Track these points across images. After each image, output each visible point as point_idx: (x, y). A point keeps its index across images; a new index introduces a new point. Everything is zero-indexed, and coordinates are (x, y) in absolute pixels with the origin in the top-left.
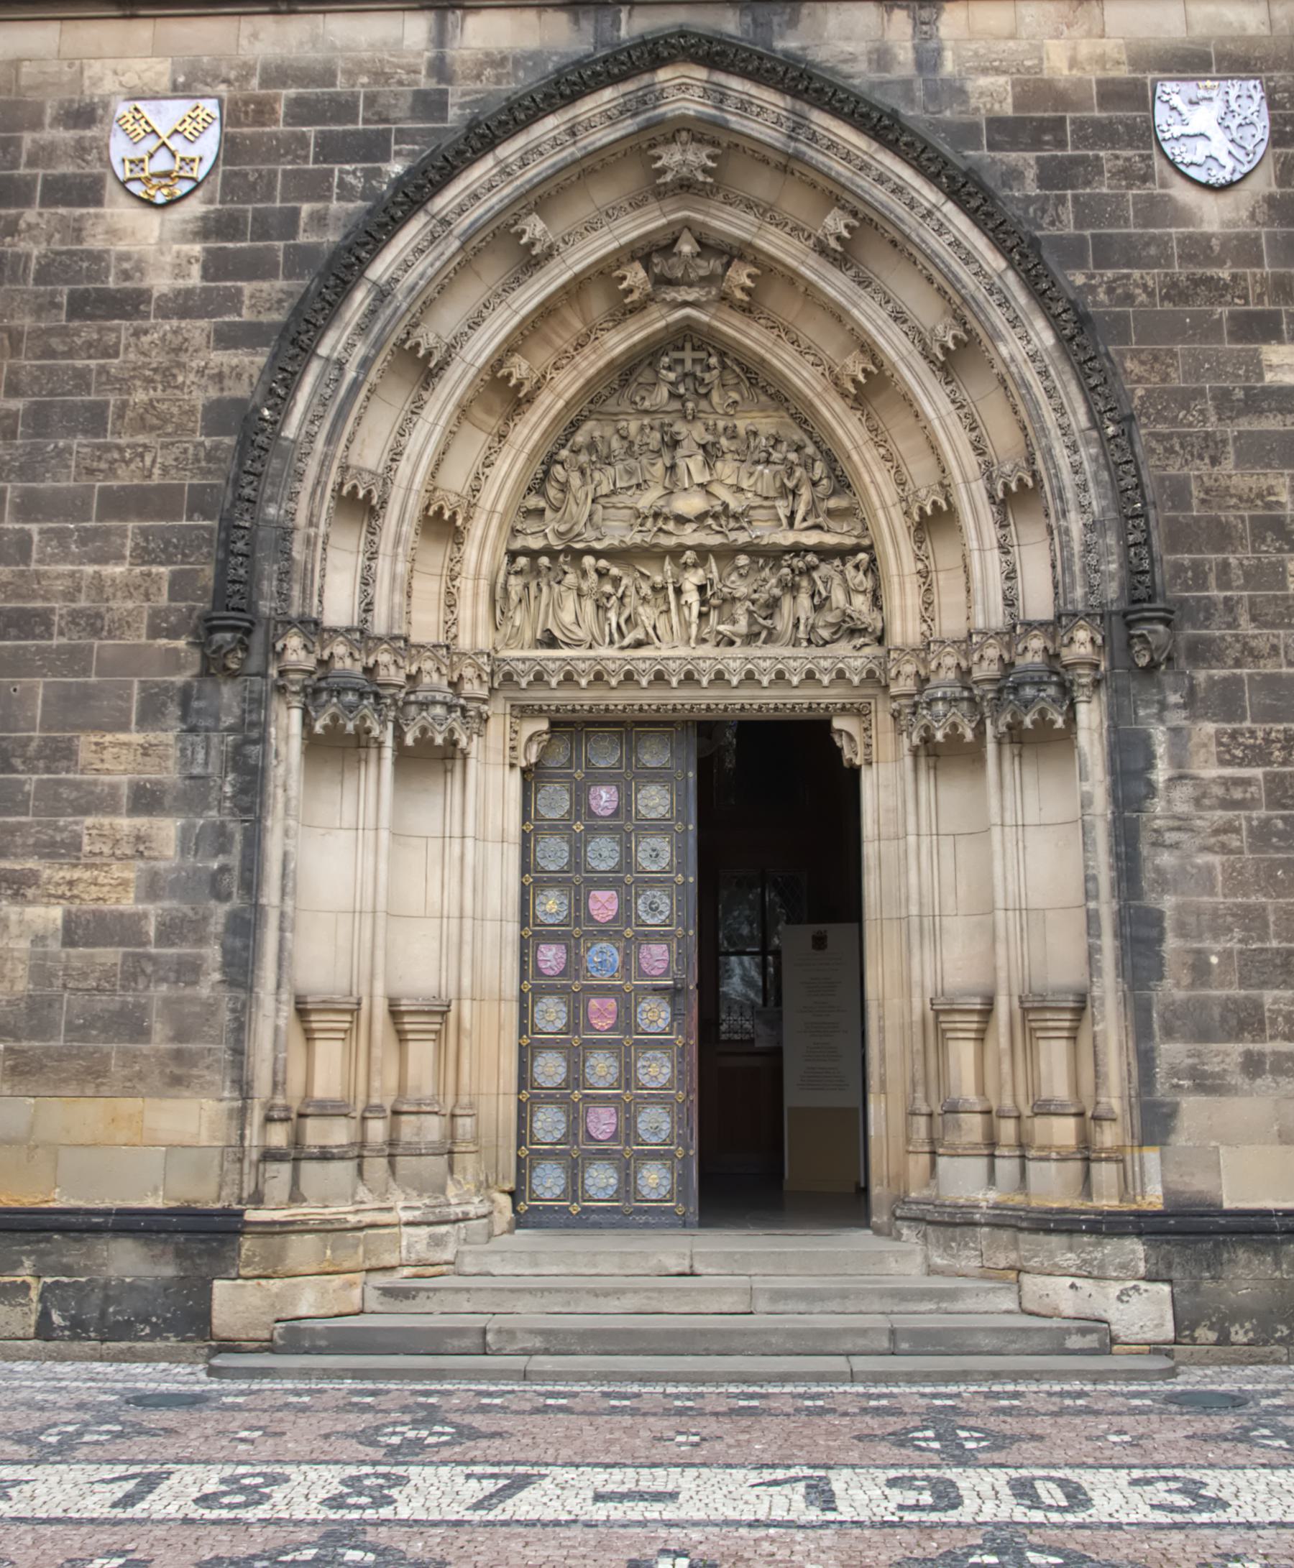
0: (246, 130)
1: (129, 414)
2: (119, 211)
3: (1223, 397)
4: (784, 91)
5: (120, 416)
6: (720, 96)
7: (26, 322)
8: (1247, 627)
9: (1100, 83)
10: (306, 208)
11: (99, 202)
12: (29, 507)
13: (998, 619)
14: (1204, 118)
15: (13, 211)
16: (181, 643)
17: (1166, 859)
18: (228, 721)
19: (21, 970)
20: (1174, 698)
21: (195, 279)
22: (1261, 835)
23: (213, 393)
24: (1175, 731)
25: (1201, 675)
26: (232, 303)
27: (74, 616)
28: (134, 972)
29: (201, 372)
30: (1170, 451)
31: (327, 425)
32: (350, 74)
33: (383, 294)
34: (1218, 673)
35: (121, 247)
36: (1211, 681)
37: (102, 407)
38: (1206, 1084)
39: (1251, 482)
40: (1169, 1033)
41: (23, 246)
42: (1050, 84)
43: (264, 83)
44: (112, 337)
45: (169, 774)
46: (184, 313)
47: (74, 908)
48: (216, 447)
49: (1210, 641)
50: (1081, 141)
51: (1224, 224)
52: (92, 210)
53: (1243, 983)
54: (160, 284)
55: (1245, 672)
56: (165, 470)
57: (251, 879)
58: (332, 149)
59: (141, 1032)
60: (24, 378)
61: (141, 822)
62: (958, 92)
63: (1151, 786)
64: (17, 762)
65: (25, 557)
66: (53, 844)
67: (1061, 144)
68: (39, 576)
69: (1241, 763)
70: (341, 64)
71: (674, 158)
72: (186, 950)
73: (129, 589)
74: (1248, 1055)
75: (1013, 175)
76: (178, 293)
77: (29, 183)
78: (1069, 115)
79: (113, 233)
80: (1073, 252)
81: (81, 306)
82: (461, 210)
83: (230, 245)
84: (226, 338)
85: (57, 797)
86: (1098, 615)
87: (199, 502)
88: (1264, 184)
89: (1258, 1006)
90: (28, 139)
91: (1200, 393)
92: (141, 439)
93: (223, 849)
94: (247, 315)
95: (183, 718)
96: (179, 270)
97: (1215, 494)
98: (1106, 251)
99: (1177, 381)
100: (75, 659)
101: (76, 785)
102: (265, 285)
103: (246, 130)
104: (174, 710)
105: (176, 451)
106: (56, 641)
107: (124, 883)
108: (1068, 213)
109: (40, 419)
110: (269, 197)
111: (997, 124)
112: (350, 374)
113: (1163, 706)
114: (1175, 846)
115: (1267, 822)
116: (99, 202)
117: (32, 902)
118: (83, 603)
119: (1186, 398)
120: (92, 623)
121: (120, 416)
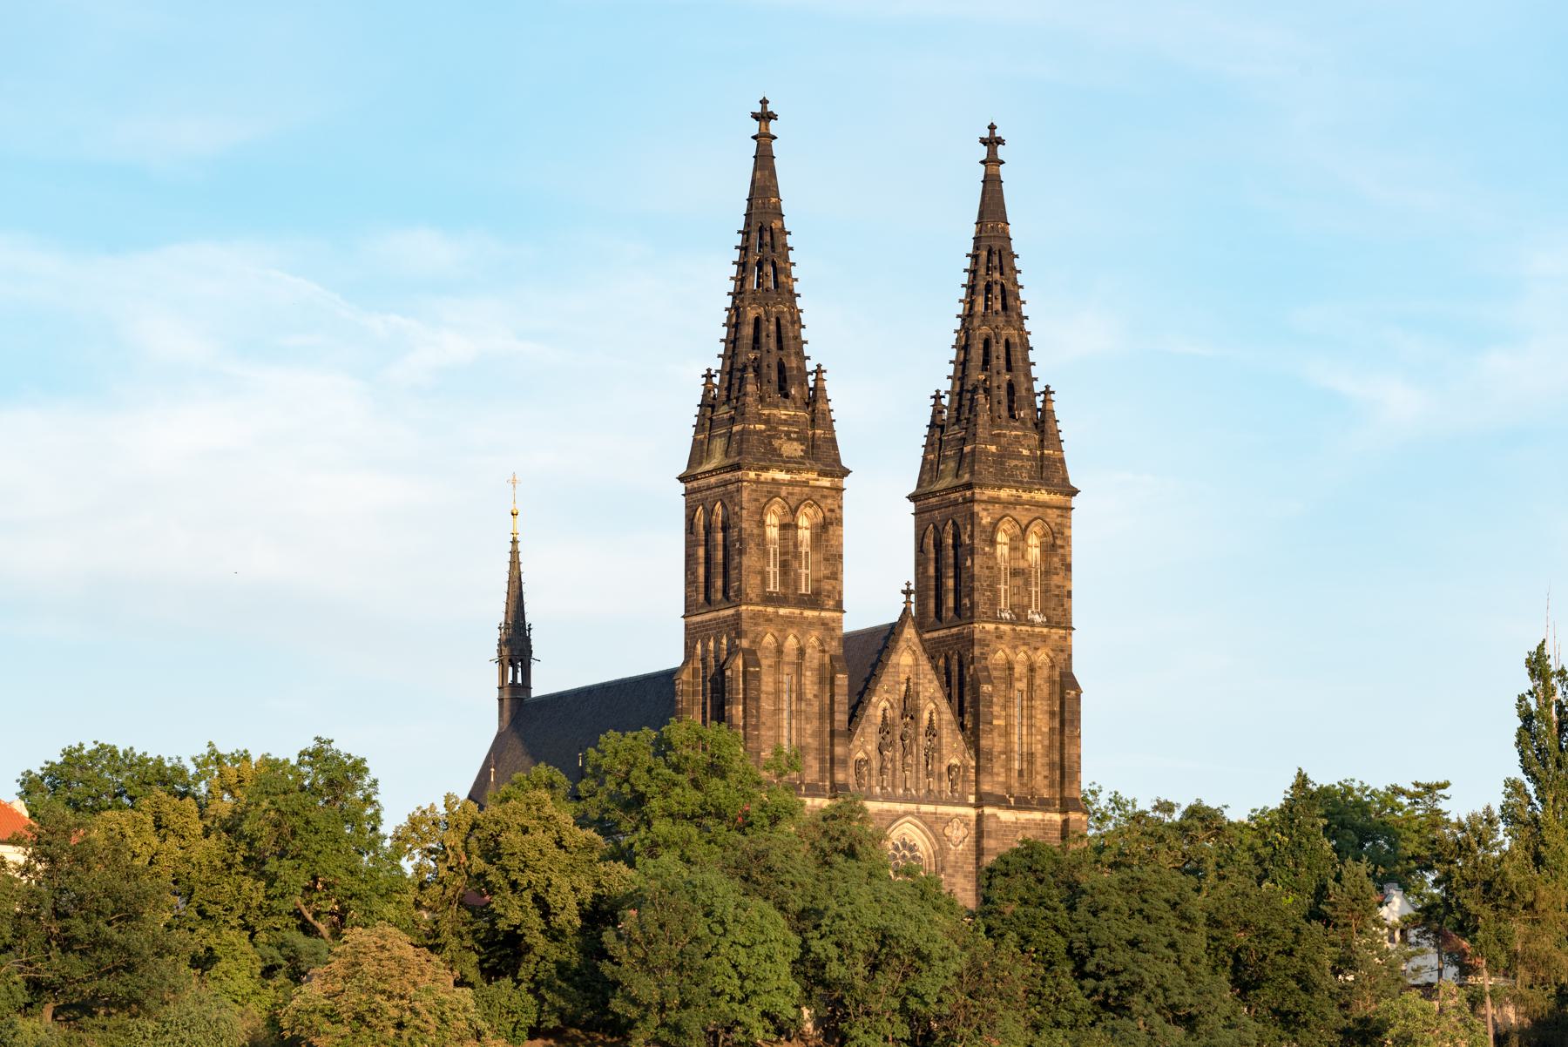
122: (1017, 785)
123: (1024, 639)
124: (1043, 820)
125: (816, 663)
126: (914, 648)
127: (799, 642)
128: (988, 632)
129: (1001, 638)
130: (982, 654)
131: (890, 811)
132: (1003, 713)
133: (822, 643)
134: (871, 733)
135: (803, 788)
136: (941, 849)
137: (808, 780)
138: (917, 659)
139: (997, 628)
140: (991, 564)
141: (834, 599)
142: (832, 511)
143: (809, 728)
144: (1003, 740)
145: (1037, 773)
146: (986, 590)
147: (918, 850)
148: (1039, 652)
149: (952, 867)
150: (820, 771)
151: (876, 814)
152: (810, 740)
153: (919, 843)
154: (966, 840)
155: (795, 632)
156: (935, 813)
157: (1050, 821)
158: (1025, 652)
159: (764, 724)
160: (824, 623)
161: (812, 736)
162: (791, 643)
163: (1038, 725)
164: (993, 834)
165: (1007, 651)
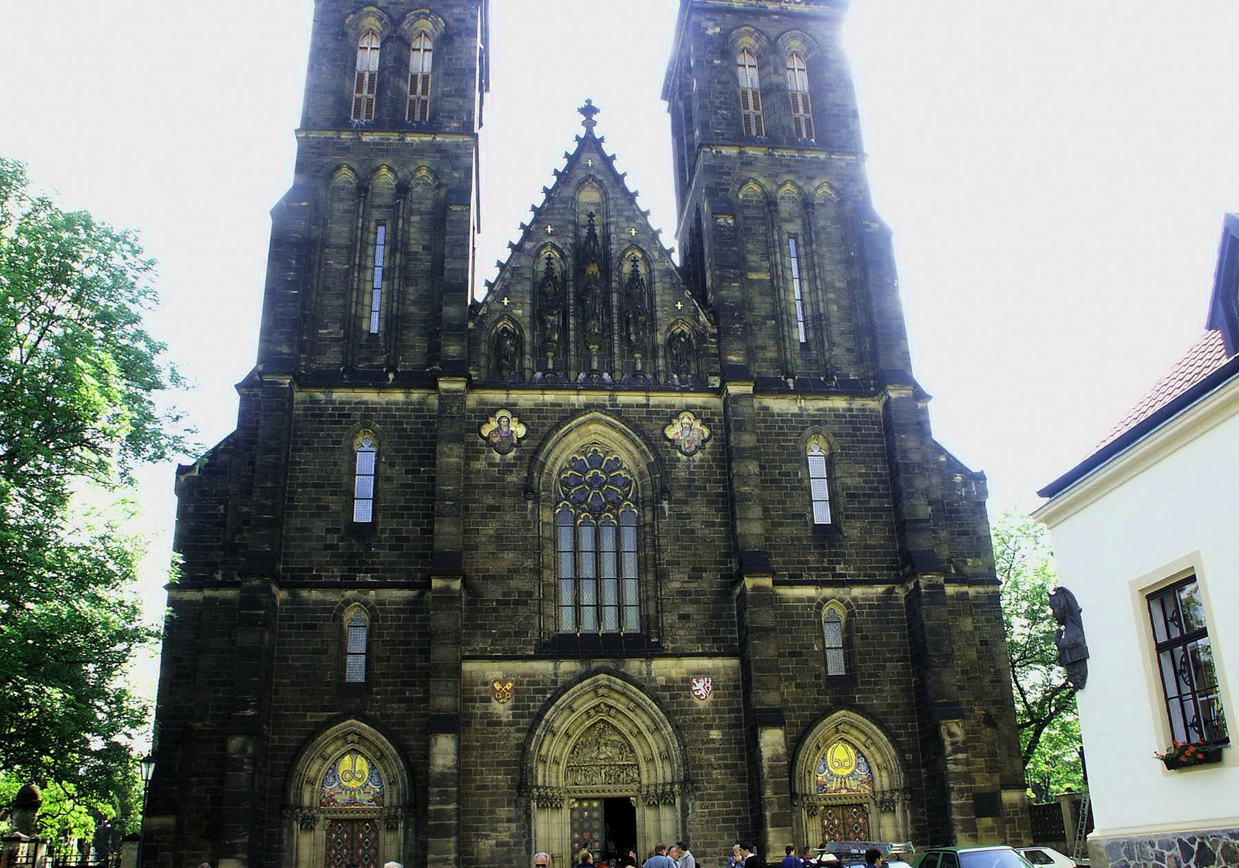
2: (495, 703)
4: (622, 680)
6: (609, 680)
8: (706, 784)
12: (483, 765)
13: (662, 782)
14: (700, 686)
16: (514, 791)
21: (511, 718)
22: (707, 822)
25: (697, 793)
26: (519, 723)
28: (509, 852)
33: (547, 721)
43: (522, 677)
45: (513, 815)
54: (504, 719)
57: (530, 836)
58: (537, 691)
59: (512, 863)
62: (655, 680)
71: (601, 691)
73: (503, 781)
75: (665, 697)
79: (494, 709)
80: (676, 713)
81: (489, 724)
84: (518, 731)
86: (680, 783)
87: (515, 763)
88: (710, 698)
90: (475, 688)
91: (698, 740)
98: (682, 713)
100: (493, 794)
108: (675, 705)
109: (483, 747)
111: (661, 686)
119: (696, 741)
120: (496, 787)
122: (799, 362)
123: (788, 166)
124: (851, 410)
125: (427, 205)
126: (599, 177)
127: (396, 175)
128: (728, 157)
129: (751, 164)
130: (720, 184)
131: (560, 405)
132: (766, 264)
133: (436, 174)
134: (522, 292)
135: (391, 376)
136: (659, 459)
137: (404, 365)
138: (606, 193)
139: (741, 153)
140: (724, 78)
141: (459, 119)
142: (463, 21)
143: (412, 292)
144: (768, 300)
145: (834, 344)
146: (720, 108)
147: (620, 468)
148: (816, 183)
149: (681, 488)
150: (429, 352)
151: (531, 410)
152: (412, 309)
153: (623, 456)
154: (708, 445)
155: (389, 162)
156: (647, 405)
157: (863, 410)
158: (793, 183)
159: (329, 289)
160: (440, 150)
161: (414, 303)
162: (385, 179)
163: (828, 279)
164: (749, 427)
165: (762, 180)
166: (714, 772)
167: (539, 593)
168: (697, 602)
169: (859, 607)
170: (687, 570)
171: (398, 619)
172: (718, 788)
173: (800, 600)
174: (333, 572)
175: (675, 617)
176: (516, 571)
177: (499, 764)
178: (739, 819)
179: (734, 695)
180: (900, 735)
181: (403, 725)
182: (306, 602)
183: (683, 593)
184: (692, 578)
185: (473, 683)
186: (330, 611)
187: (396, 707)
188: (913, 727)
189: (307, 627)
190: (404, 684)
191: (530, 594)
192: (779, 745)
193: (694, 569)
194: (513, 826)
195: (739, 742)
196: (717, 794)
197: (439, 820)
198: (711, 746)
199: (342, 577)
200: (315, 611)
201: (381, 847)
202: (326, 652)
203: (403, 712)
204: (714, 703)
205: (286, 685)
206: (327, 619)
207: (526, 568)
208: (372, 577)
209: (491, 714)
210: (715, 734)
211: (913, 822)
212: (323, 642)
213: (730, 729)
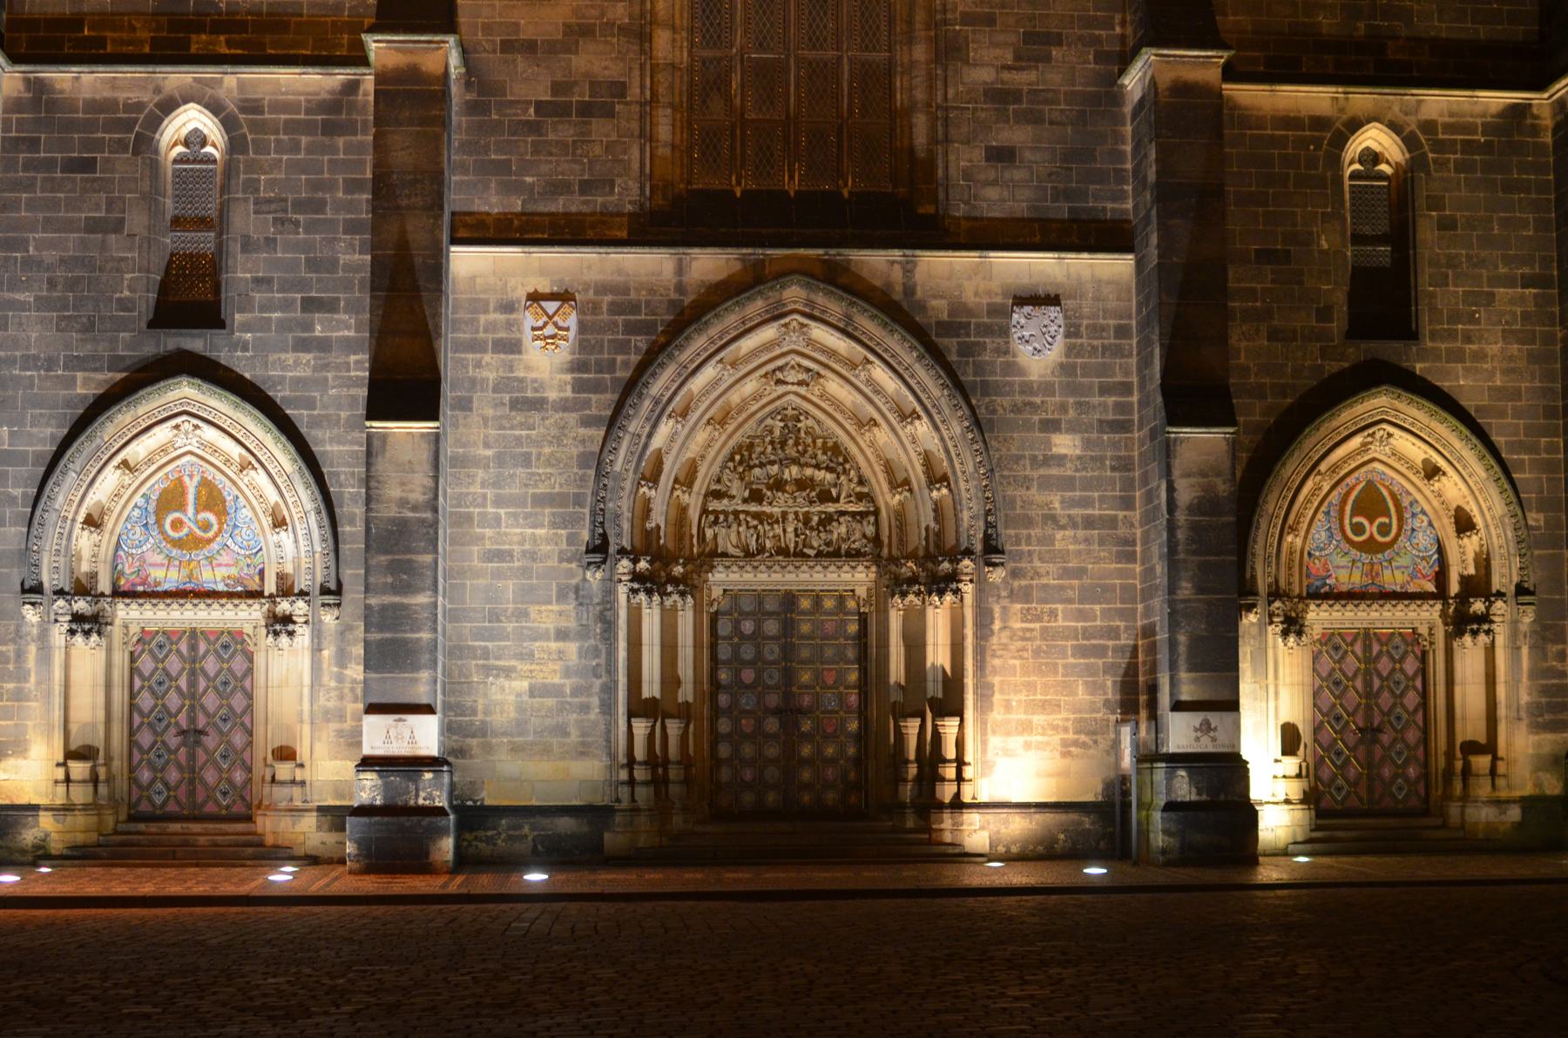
0: (589, 318)
1: (542, 458)
3: (1034, 459)
5: (539, 459)
7: (490, 412)
8: (1037, 563)
9: (988, 304)
10: (619, 358)
11: (520, 352)
12: (499, 502)
15: (478, 356)
16: (574, 565)
17: (997, 662)
18: (596, 600)
19: (512, 708)
20: (1004, 594)
21: (569, 393)
23: (581, 449)
24: (1004, 608)
25: (1016, 584)
27: (524, 553)
28: (561, 708)
29: (575, 439)
30: (1009, 483)
31: (634, 464)
32: (637, 290)
34: (1023, 583)
35: (534, 375)
36: (1020, 587)
37: (530, 454)
38: (1007, 753)
39: (1044, 498)
40: (994, 732)
41: (485, 374)
42: (965, 304)
43: (596, 293)
44: (531, 421)
45: (572, 624)
46: (565, 409)
47: (533, 681)
48: (584, 475)
49: (1021, 569)
50: (978, 334)
51: (1040, 376)
52: (517, 356)
53: (1025, 712)
54: (552, 395)
55: (1034, 582)
56: (561, 485)
60: (492, 440)
61: (561, 645)
62: (922, 307)
63: (992, 631)
64: (503, 618)
65: (499, 525)
66: (521, 654)
67: (968, 335)
68: (506, 534)
69: (1031, 621)
70: (632, 284)
72: (583, 699)
73: (548, 541)
74: (1026, 742)
76: (561, 399)
77: (485, 342)
78: (973, 320)
79: (528, 368)
81: (515, 404)
82: (692, 361)
83: (585, 376)
84: (587, 422)
85: (522, 634)
87: (578, 500)
89: (1030, 722)
90: (483, 318)
92: (548, 470)
93: (597, 656)
94: (594, 411)
95: (577, 599)
96: (561, 389)
97: (1027, 503)
99: (1014, 451)
101: (531, 629)
102: (602, 397)
103: (589, 318)
104: (572, 595)
105: (565, 476)
106: (516, 564)
107: (555, 671)
108: (970, 370)
109: (500, 459)
110: (601, 352)
111: (939, 324)
112: (643, 439)
113: (999, 597)
114: (1001, 656)
115: (1039, 647)
116: (520, 352)
117: (515, 679)
118: (527, 547)
120: (532, 556)
121: (539, 459)
166: (1059, 535)
167: (642, 87)
168: (1033, 118)
169: (1439, 146)
170: (1012, 38)
171: (296, 148)
172: (1066, 573)
173: (1290, 121)
174: (133, 29)
175: (978, 154)
176: (586, 31)
177: (540, 501)
178: (1115, 649)
179: (1118, 352)
180: (1520, 466)
181: (310, 404)
182: (70, 105)
183: (1001, 97)
184: (1022, 60)
185: (479, 306)
186: (128, 125)
187: (291, 362)
188: (1552, 449)
189: (73, 166)
190: (310, 305)
191: (619, 89)
192: (1218, 475)
193: (1029, 37)
194: (572, 648)
195: (1123, 465)
196: (1062, 588)
197: (393, 628)
198: (1054, 471)
199: (155, 42)
200: (90, 126)
201: (259, 694)
202: (118, 227)
203: (309, 373)
204: (1066, 369)
205: (23, 306)
206: (121, 146)
207: (611, 24)
208: (229, 44)
209: (521, 380)
210: (1065, 444)
211: (1534, 674)
212: (110, 204)
213: (1102, 431)
